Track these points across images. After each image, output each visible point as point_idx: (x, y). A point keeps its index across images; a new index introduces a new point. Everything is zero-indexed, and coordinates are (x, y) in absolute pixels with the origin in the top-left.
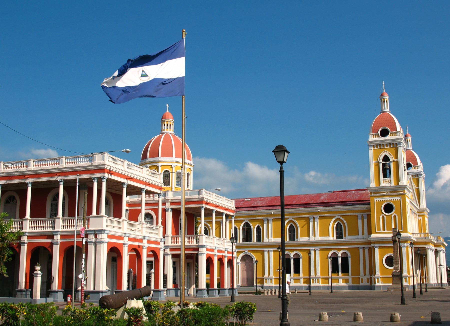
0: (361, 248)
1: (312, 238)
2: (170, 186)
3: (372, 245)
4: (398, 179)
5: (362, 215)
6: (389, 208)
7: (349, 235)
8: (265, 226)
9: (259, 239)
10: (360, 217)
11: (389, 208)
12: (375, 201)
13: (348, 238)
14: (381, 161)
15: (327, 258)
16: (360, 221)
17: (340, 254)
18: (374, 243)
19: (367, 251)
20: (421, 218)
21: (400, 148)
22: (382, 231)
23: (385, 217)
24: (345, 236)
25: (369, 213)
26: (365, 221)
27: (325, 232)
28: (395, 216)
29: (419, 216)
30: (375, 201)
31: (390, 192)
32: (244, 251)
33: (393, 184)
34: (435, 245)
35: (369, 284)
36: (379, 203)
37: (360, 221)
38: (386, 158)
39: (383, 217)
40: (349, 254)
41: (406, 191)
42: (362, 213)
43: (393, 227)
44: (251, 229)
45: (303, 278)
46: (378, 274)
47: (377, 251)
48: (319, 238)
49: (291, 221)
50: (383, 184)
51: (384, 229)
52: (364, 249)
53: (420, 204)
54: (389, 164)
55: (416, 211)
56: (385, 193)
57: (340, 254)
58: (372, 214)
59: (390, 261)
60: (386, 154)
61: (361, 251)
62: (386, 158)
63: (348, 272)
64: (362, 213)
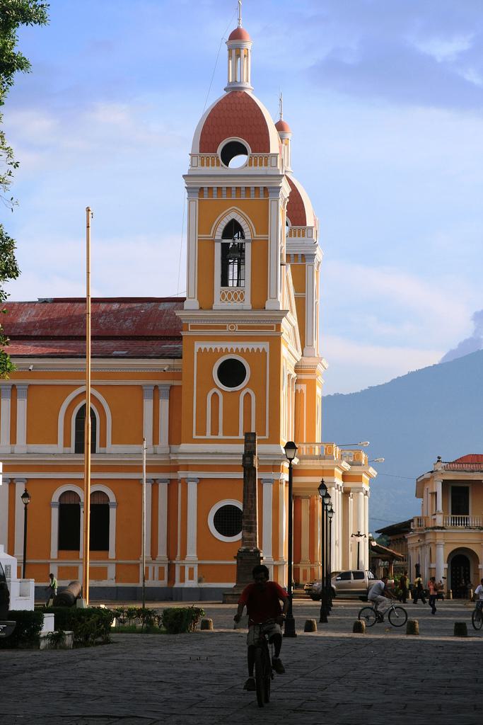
3: (181, 475)
5: (156, 387)
6: (232, 373)
7: (113, 443)
12: (196, 350)
14: (219, 235)
15: (50, 505)
16: (148, 405)
18: (187, 468)
19: (163, 488)
22: (209, 436)
25: (176, 383)
26: (164, 404)
30: (196, 350)
31: (240, 328)
35: (163, 583)
36: (207, 356)
37: (148, 405)
38: (233, 228)
40: (112, 499)
46: (192, 554)
47: (192, 488)
51: (215, 432)
52: (154, 483)
56: (225, 327)
59: (229, 521)
60: (233, 216)
62: (233, 228)
63: (106, 548)
64: (157, 382)
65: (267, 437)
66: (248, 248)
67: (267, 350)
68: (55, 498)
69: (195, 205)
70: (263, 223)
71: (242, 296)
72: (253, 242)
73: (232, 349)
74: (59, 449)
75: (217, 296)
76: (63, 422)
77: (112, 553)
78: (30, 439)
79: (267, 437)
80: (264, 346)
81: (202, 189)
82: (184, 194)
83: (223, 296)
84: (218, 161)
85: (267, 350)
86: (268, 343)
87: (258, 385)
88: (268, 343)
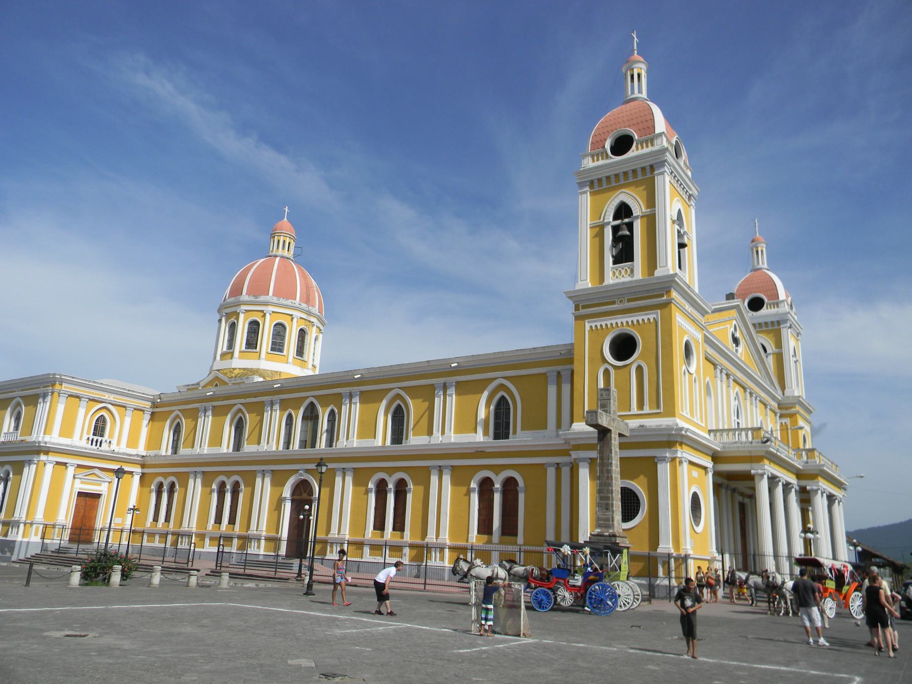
0: (550, 465)
1: (437, 438)
4: (652, 261)
7: (523, 429)
8: (345, 409)
9: (330, 443)
10: (553, 377)
11: (624, 347)
13: (520, 438)
16: (552, 390)
19: (566, 471)
20: (787, 421)
21: (660, 177)
23: (612, 371)
24: (515, 432)
26: (566, 388)
27: (467, 423)
28: (640, 369)
29: (781, 416)
31: (629, 301)
32: (297, 471)
33: (639, 275)
34: (799, 475)
37: (552, 390)
38: (623, 211)
39: (606, 372)
40: (521, 483)
41: (674, 294)
42: (559, 368)
43: (601, 385)
44: (317, 417)
45: (452, 548)
49: (398, 396)
50: (610, 279)
52: (558, 467)
53: (783, 388)
54: (630, 226)
55: (775, 405)
56: (614, 303)
58: (576, 367)
61: (551, 472)
62: (623, 211)
63: (516, 535)
64: (559, 368)
73: (622, 323)
77: (520, 539)
84: (607, 155)
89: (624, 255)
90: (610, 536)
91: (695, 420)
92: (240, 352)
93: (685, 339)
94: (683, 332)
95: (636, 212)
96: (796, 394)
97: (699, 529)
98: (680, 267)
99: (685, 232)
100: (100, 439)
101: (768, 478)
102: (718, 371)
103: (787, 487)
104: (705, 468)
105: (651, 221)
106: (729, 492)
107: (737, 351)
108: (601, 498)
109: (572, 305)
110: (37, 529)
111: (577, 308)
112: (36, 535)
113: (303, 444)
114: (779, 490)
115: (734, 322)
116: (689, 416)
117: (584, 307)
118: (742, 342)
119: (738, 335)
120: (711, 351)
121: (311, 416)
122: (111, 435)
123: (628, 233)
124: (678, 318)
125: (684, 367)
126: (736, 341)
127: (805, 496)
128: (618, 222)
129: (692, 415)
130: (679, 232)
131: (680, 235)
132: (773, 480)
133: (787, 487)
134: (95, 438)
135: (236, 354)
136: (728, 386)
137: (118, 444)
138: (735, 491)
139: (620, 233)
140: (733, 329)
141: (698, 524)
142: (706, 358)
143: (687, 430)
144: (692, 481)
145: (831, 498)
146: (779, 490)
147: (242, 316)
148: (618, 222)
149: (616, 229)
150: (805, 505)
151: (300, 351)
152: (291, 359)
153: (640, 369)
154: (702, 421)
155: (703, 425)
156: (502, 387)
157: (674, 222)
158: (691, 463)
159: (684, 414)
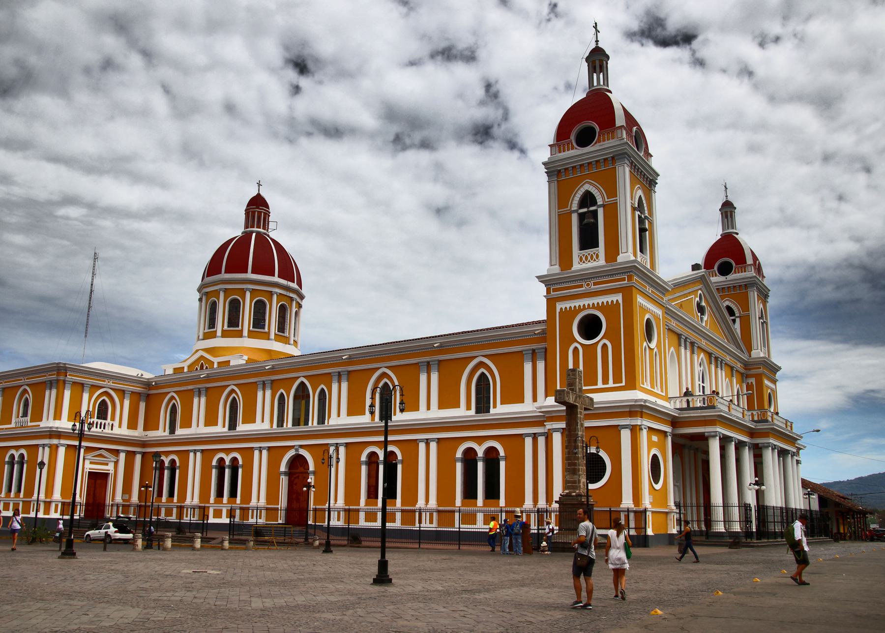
0: (528, 435)
2: (266, 330)
8: (335, 386)
9: (321, 420)
11: (590, 327)
12: (558, 310)
14: (575, 207)
17: (480, 451)
19: (541, 440)
21: (621, 169)
24: (495, 407)
26: (541, 366)
27: (448, 399)
29: (748, 376)
30: (558, 310)
32: (293, 447)
33: (602, 261)
34: (752, 433)
38: (588, 199)
39: (576, 350)
40: (502, 453)
43: (571, 366)
48: (436, 414)
52: (535, 437)
53: (749, 349)
54: (595, 213)
56: (581, 286)
57: (480, 451)
60: (587, 187)
61: (528, 441)
62: (588, 199)
63: (498, 497)
64: (534, 346)
65: (623, 384)
66: (601, 212)
67: (621, 302)
68: (459, 454)
69: (555, 185)
70: (612, 189)
71: (597, 256)
72: (603, 206)
73: (588, 305)
74: (463, 412)
75: (576, 259)
76: (465, 389)
77: (502, 502)
78: (441, 406)
79: (623, 384)
80: (618, 298)
81: (559, 171)
82: (545, 178)
83: (581, 259)
85: (621, 302)
86: (621, 295)
87: (613, 335)
88: (621, 295)
89: (589, 240)
90: (577, 496)
91: (655, 391)
92: (223, 331)
93: (647, 316)
94: (645, 310)
95: (600, 201)
96: (762, 355)
97: (658, 487)
98: (641, 251)
99: (646, 217)
100: (103, 422)
101: (720, 439)
102: (683, 341)
103: (740, 445)
104: (665, 433)
105: (612, 211)
106: (692, 452)
107: (702, 319)
108: (569, 464)
109: (543, 289)
110: (57, 506)
111: (548, 291)
112: (56, 511)
113: (296, 423)
114: (732, 448)
115: (700, 292)
116: (649, 388)
117: (555, 290)
118: (707, 310)
119: (703, 304)
120: (673, 324)
121: (302, 395)
122: (113, 419)
123: (592, 220)
124: (639, 299)
125: (645, 344)
126: (701, 309)
127: (758, 452)
128: (585, 210)
129: (652, 387)
130: (639, 217)
131: (641, 221)
132: (725, 441)
133: (740, 445)
134: (99, 421)
135: (219, 333)
136: (693, 352)
137: (120, 426)
138: (690, 451)
139: (586, 221)
140: (698, 299)
141: (657, 482)
142: (669, 330)
143: (645, 401)
144: (651, 444)
145: (783, 453)
146: (732, 448)
147: (222, 295)
148: (585, 210)
149: (582, 217)
150: (758, 459)
151: (281, 327)
152: (272, 336)
153: (605, 345)
154: (662, 391)
155: (664, 394)
156: (481, 364)
157: (634, 209)
158: (650, 429)
159: (645, 386)
